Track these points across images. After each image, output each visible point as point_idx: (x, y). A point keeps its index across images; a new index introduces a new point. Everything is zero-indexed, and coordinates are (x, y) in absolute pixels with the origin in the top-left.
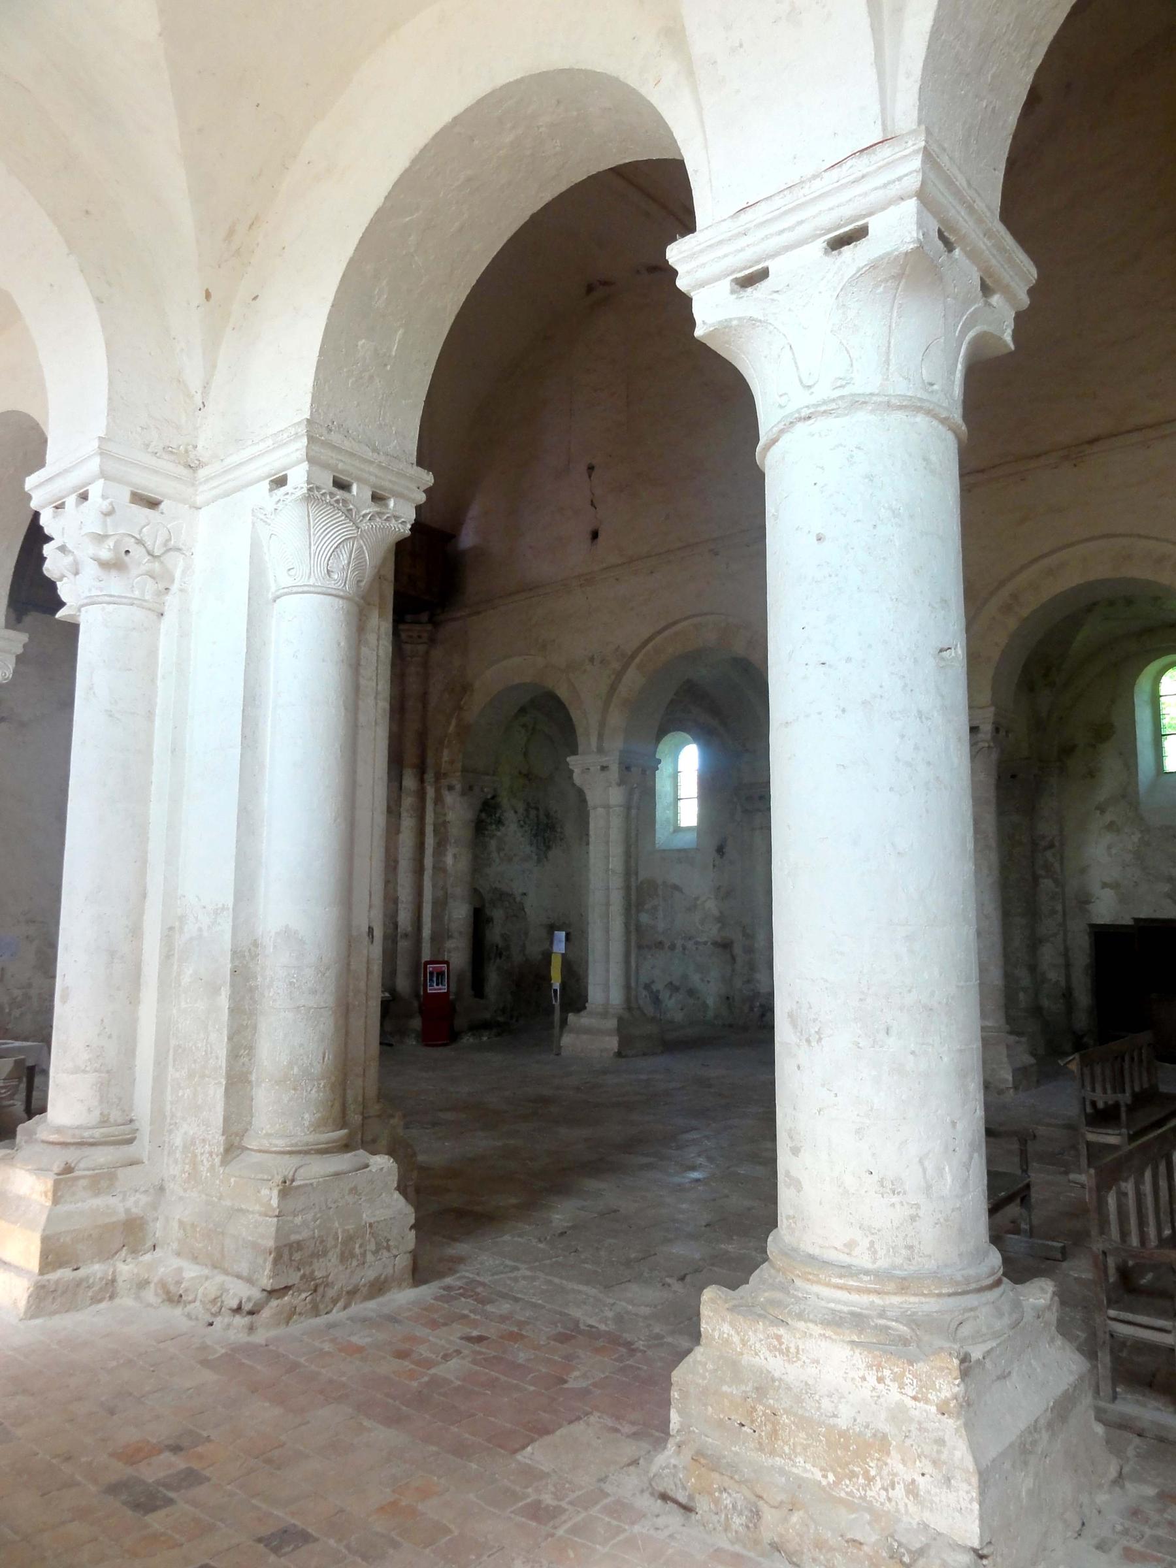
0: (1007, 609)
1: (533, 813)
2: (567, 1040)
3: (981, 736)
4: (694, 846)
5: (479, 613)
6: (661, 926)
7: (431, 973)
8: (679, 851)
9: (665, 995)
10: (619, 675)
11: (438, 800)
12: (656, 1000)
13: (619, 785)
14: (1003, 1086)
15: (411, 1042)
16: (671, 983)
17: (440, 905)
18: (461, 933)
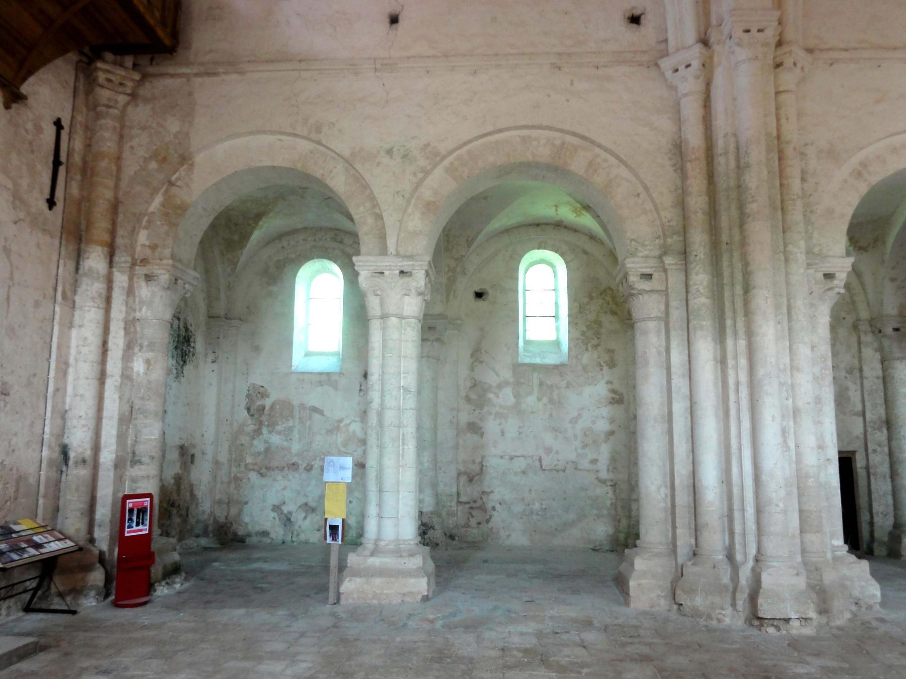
0: (858, 175)
1: (176, 322)
2: (349, 586)
3: (836, 282)
4: (337, 370)
5: (215, 74)
6: (296, 447)
7: (131, 511)
8: (321, 374)
9: (298, 517)
10: (427, 173)
11: (130, 291)
12: (287, 521)
13: (420, 294)
14: (871, 602)
15: (89, 603)
16: (306, 504)
17: (126, 419)
18: (153, 458)
